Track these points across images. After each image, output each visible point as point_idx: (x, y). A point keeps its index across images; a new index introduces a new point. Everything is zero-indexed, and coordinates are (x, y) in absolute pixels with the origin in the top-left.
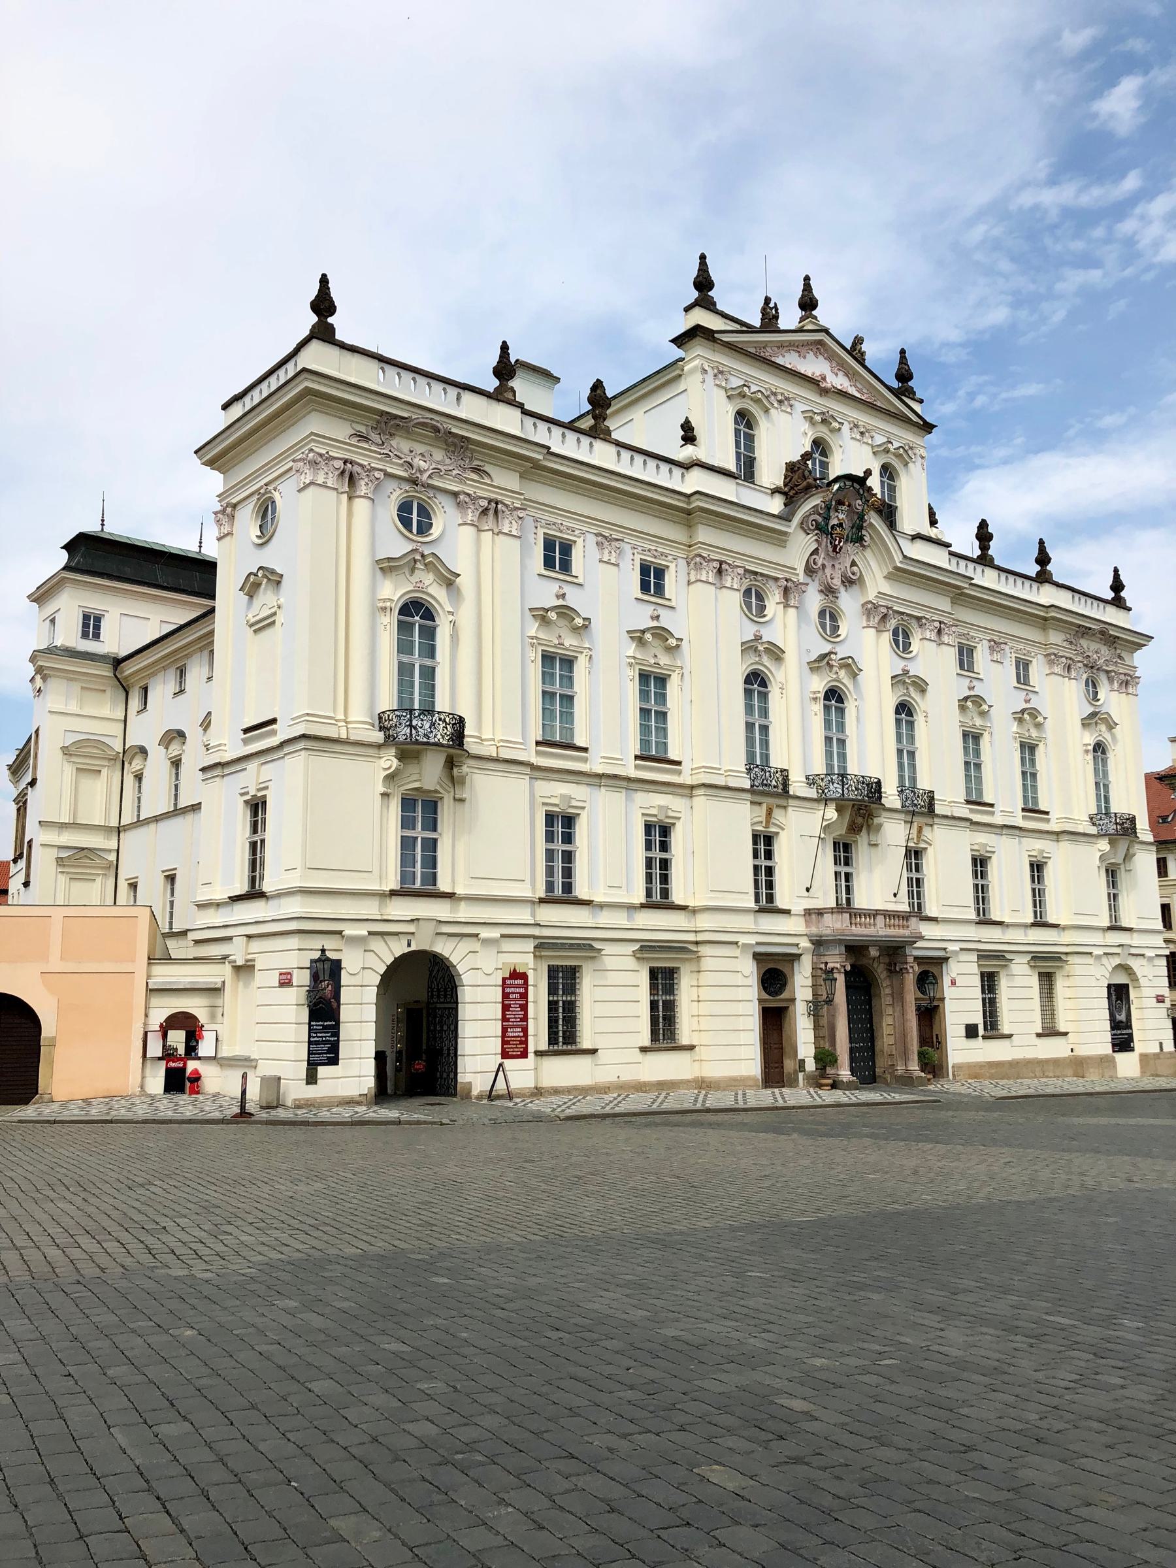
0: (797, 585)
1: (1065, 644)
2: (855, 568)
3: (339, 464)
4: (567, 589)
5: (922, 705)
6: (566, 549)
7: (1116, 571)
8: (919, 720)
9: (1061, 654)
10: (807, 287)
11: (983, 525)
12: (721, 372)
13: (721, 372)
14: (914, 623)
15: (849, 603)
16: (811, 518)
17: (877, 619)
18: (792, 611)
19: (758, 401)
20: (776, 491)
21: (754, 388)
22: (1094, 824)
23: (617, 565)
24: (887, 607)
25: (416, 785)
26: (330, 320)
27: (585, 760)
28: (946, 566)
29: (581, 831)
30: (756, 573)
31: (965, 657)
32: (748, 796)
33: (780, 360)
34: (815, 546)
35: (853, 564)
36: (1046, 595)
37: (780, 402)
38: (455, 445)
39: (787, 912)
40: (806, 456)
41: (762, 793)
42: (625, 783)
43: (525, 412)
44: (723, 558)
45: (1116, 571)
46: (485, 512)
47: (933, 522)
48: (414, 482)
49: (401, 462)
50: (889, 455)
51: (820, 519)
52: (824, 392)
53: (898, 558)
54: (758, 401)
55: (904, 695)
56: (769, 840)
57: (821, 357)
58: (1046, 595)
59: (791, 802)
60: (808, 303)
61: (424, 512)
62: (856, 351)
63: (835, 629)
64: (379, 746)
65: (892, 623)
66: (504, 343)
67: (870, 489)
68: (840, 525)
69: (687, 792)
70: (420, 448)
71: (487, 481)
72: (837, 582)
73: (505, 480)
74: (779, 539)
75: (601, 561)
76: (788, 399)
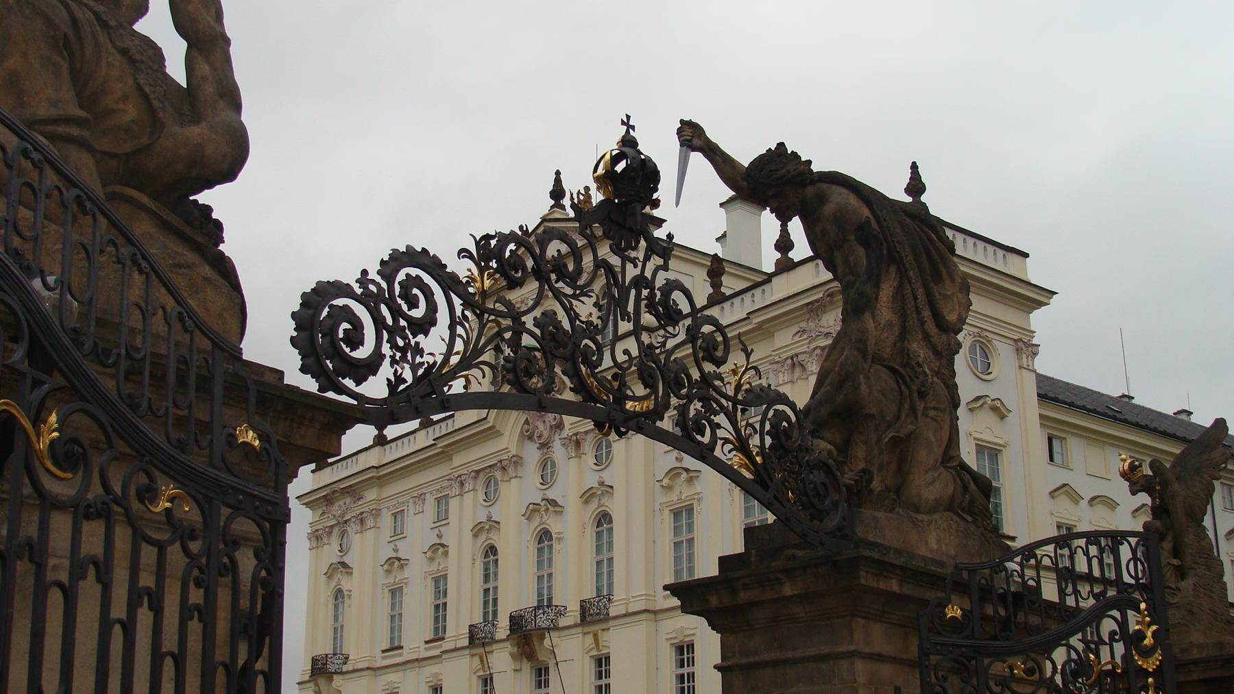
0: (510, 459)
1: (797, 338)
5: (615, 507)
7: (914, 166)
8: (616, 525)
9: (784, 356)
10: (558, 181)
24: (576, 434)
27: (401, 655)
32: (467, 652)
42: (416, 664)
45: (914, 166)
46: (362, 521)
60: (557, 193)
70: (341, 503)
72: (546, 434)
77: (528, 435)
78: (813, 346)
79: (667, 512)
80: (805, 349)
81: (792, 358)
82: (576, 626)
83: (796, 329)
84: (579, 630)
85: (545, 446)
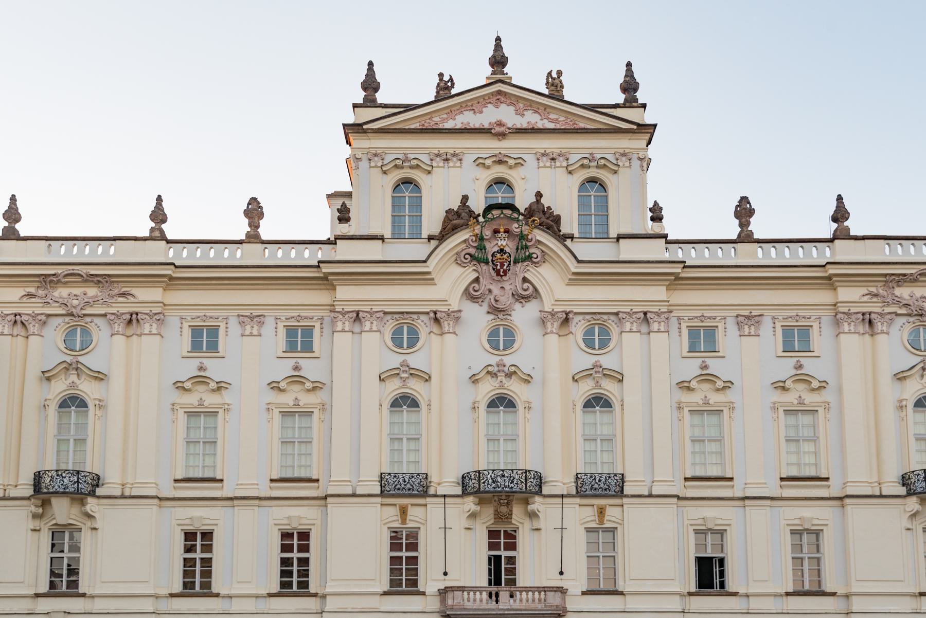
1: (866, 298)
2: (526, 285)
3: (9, 318)
4: (207, 362)
6: (213, 332)
9: (853, 310)
11: (744, 200)
12: (375, 155)
13: (375, 155)
14: (612, 317)
15: (523, 317)
16: (463, 253)
17: (556, 325)
18: (449, 338)
19: (417, 167)
20: (430, 238)
21: (412, 156)
22: (904, 485)
23: (260, 335)
24: (567, 314)
25: (54, 522)
26: (6, 224)
28: (666, 256)
29: (216, 542)
30: (402, 313)
31: (702, 339)
32: (379, 500)
33: (449, 125)
34: (476, 275)
35: (525, 280)
36: (845, 251)
37: (447, 160)
38: (99, 281)
39: (423, 594)
40: (465, 198)
41: (393, 496)
42: (257, 502)
43: (169, 242)
44: (357, 308)
46: (130, 321)
47: (657, 215)
48: (72, 315)
49: (57, 305)
50: (590, 170)
51: (472, 251)
52: (502, 136)
53: (574, 267)
54: (418, 166)
55: (594, 388)
56: (413, 535)
57: (503, 106)
58: (845, 251)
59: (429, 500)
61: (86, 332)
62: (555, 84)
63: (510, 341)
64: (28, 498)
65: (578, 327)
66: (159, 196)
67: (549, 208)
68: (502, 251)
69: (322, 502)
70: (77, 291)
71: (132, 299)
73: (147, 296)
74: (425, 278)
75: (243, 335)
76: (454, 155)
77: (471, 295)
78: (887, 310)
79: (686, 410)
80: (879, 310)
81: (863, 314)
82: (569, 496)
83: (864, 291)
84: (578, 500)
85: (495, 310)
